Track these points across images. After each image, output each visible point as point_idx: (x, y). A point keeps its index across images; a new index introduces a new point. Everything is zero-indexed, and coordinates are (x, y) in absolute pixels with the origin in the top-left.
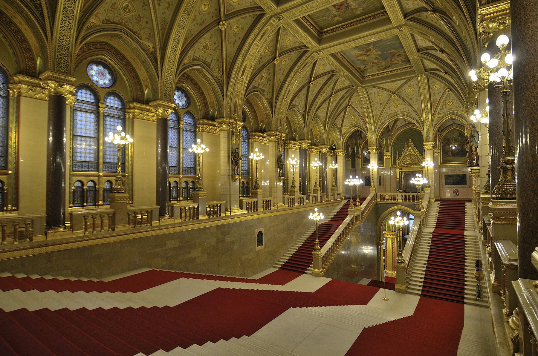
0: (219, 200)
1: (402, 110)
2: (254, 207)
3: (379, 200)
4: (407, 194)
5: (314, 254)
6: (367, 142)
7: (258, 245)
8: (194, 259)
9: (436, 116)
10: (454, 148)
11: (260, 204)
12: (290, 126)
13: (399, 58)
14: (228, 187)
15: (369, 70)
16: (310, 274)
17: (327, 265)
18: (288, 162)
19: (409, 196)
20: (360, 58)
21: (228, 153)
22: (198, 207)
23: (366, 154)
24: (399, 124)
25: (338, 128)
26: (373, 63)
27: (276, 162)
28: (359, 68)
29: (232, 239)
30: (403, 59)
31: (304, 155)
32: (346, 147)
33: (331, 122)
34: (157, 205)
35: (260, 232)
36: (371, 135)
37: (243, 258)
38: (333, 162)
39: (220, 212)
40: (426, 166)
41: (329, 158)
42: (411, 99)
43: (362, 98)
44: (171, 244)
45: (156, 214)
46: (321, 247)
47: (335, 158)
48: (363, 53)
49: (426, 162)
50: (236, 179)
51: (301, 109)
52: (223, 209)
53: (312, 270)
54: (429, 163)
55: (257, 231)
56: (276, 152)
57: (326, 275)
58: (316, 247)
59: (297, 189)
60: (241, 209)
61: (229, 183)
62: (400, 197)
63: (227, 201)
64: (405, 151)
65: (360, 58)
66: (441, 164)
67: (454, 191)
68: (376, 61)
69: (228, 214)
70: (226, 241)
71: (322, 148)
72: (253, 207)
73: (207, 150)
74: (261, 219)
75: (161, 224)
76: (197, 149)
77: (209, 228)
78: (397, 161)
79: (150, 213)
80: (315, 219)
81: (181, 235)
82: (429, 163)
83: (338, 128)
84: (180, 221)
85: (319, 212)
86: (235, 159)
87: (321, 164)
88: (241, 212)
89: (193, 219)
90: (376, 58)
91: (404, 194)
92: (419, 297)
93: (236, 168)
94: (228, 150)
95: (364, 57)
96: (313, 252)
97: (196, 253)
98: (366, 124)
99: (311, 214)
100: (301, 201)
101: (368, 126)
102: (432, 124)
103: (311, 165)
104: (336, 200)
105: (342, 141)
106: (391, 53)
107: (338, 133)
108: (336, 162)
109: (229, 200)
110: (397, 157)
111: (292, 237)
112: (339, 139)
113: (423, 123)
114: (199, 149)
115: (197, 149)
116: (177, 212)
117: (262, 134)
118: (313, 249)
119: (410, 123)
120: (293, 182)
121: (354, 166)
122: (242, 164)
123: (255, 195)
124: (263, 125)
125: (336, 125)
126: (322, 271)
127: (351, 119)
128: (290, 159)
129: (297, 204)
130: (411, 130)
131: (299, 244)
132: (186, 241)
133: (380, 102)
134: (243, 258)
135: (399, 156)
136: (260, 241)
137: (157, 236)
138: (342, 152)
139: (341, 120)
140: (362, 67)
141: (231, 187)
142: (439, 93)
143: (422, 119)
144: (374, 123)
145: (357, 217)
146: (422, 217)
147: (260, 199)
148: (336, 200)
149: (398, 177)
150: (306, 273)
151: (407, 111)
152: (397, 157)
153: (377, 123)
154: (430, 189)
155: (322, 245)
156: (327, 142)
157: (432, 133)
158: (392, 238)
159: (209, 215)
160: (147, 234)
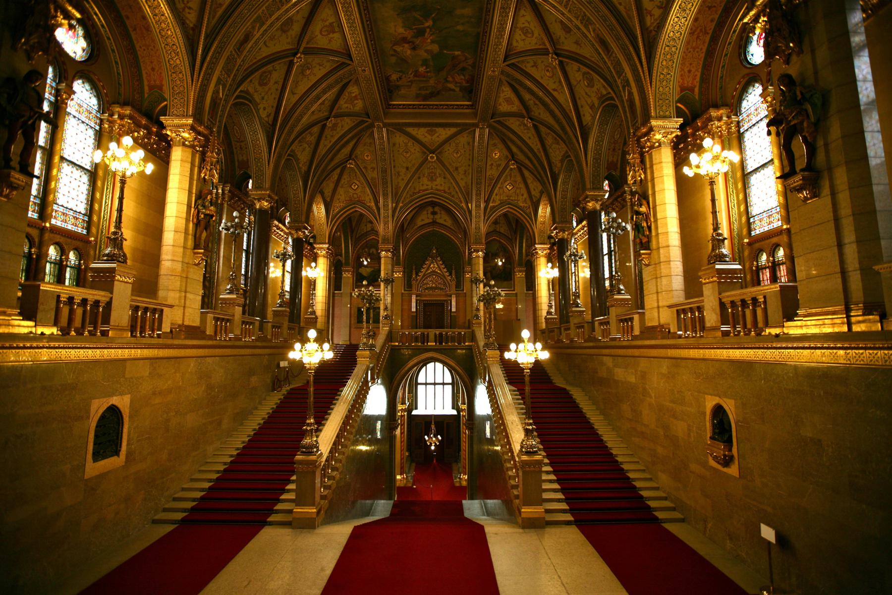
1: (438, 187)
7: (98, 456)
9: (491, 204)
10: (500, 263)
11: (121, 314)
12: (232, 153)
13: (458, 78)
15: (403, 92)
20: (399, 49)
24: (419, 223)
26: (417, 74)
28: (388, 79)
30: (464, 84)
36: (386, 223)
42: (457, 169)
43: (378, 147)
48: (408, 34)
51: (263, 114)
55: (98, 407)
65: (399, 49)
68: (422, 69)
88: (24, 327)
90: (425, 63)
95: (406, 50)
98: (377, 202)
99: (298, 346)
106: (454, 57)
111: (219, 423)
113: (470, 212)
127: (351, 191)
133: (405, 165)
135: (417, 274)
139: (332, 186)
140: (394, 77)
142: (499, 165)
150: (271, 524)
151: (446, 189)
157: (483, 229)
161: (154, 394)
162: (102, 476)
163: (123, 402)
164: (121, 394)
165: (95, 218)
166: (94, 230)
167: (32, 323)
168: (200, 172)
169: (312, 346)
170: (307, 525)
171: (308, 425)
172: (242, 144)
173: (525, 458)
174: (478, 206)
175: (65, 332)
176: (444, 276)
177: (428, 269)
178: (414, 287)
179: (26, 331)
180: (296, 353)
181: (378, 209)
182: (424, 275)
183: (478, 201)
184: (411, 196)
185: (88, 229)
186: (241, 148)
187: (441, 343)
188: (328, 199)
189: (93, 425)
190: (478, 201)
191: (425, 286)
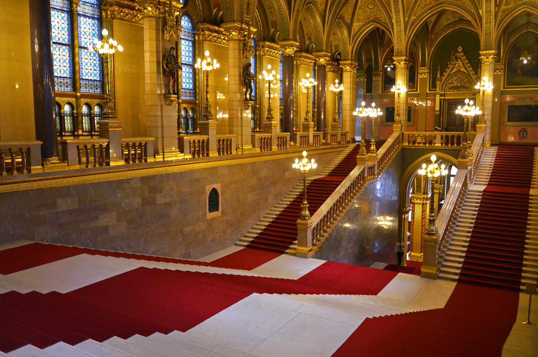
0: (145, 135)
2: (203, 150)
3: (406, 144)
4: (450, 133)
5: (300, 224)
6: (392, 50)
7: (211, 210)
8: (105, 229)
9: (503, 7)
10: (525, 62)
11: (213, 145)
12: (266, 17)
14: (159, 114)
16: (295, 255)
17: (319, 240)
18: (260, 77)
19: (453, 137)
21: (158, 56)
22: (108, 146)
23: (389, 69)
24: (444, 21)
25: (346, 23)
27: (240, 76)
29: (168, 200)
31: (289, 67)
32: (358, 57)
33: (335, 12)
34: (38, 139)
35: (214, 192)
36: (399, 37)
37: (187, 229)
38: (337, 81)
39: (146, 155)
40: (482, 89)
41: (330, 75)
44: (65, 204)
45: (36, 153)
46: (312, 215)
47: (340, 75)
49: (483, 83)
50: (172, 101)
52: (150, 150)
53: (295, 249)
54: (486, 85)
55: (208, 189)
56: (240, 59)
57: (318, 256)
58: (303, 213)
59: (276, 122)
60: (182, 151)
61: (159, 108)
62: (438, 139)
63: (157, 138)
64: (451, 66)
66: (504, 88)
67: (520, 131)
69: (159, 158)
70: (158, 202)
71: (319, 57)
72: (201, 150)
73: (121, 48)
74: (216, 168)
75: (46, 171)
76: (102, 47)
77: (128, 181)
78: (438, 83)
79: (27, 153)
80: (302, 169)
81: (81, 189)
82: (486, 85)
83: (346, 23)
84: (78, 167)
85: (309, 157)
86: (170, 66)
87: (316, 83)
88: (181, 156)
89: (101, 164)
91: (445, 133)
92: (454, 284)
93: (171, 83)
94: (158, 51)
96: (299, 221)
97: (107, 220)
98: (391, 18)
99: (297, 160)
100: (282, 143)
101: (394, 21)
102: (496, 21)
103: (300, 84)
104: (339, 143)
105: (351, 47)
107: (346, 33)
108: (341, 82)
109: (160, 135)
110: (438, 76)
111: (267, 199)
112: (347, 42)
114: (106, 46)
115: (102, 47)
116: (72, 154)
117: (217, 28)
118: (298, 217)
119: (462, 20)
120: (270, 110)
121: (369, 89)
122: (185, 78)
123: (205, 130)
124: (218, 12)
125: (342, 18)
126: (311, 250)
127: (367, 10)
128: (264, 72)
129: (275, 148)
130: (461, 32)
131: (278, 210)
132: (90, 202)
134: (187, 229)
135: (442, 75)
136: (214, 205)
137: (41, 191)
138: (351, 64)
139: (351, 10)
141: (164, 114)
143: (480, 11)
144: (404, 17)
145: (371, 168)
146: (470, 168)
147: (213, 137)
148: (339, 143)
149: (437, 108)
150: (287, 253)
152: (438, 76)
153: (409, 18)
154: (484, 125)
155: (312, 211)
156: (327, 46)
158: (423, 204)
159: (127, 160)
160: (23, 187)
161: (231, 183)
162: (213, 219)
163: (218, 186)
164: (217, 183)
165: (197, 90)
166: (198, 97)
167: (183, 154)
168: (244, 53)
169: (305, 160)
170: (304, 256)
171: (303, 204)
172: (272, 9)
173: (427, 236)
174: (488, 12)
175: (193, 155)
176: (469, 74)
177: (453, 68)
178: (438, 89)
179: (181, 158)
180: (297, 165)
181: (392, 25)
182: (449, 75)
183: (488, 6)
184: (423, 8)
185: (195, 97)
186: (271, 12)
187: (447, 144)
188: (349, 22)
189: (208, 196)
190: (488, 6)
191: (450, 86)
